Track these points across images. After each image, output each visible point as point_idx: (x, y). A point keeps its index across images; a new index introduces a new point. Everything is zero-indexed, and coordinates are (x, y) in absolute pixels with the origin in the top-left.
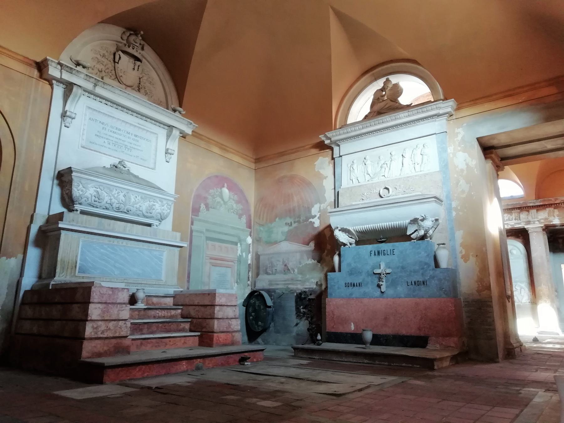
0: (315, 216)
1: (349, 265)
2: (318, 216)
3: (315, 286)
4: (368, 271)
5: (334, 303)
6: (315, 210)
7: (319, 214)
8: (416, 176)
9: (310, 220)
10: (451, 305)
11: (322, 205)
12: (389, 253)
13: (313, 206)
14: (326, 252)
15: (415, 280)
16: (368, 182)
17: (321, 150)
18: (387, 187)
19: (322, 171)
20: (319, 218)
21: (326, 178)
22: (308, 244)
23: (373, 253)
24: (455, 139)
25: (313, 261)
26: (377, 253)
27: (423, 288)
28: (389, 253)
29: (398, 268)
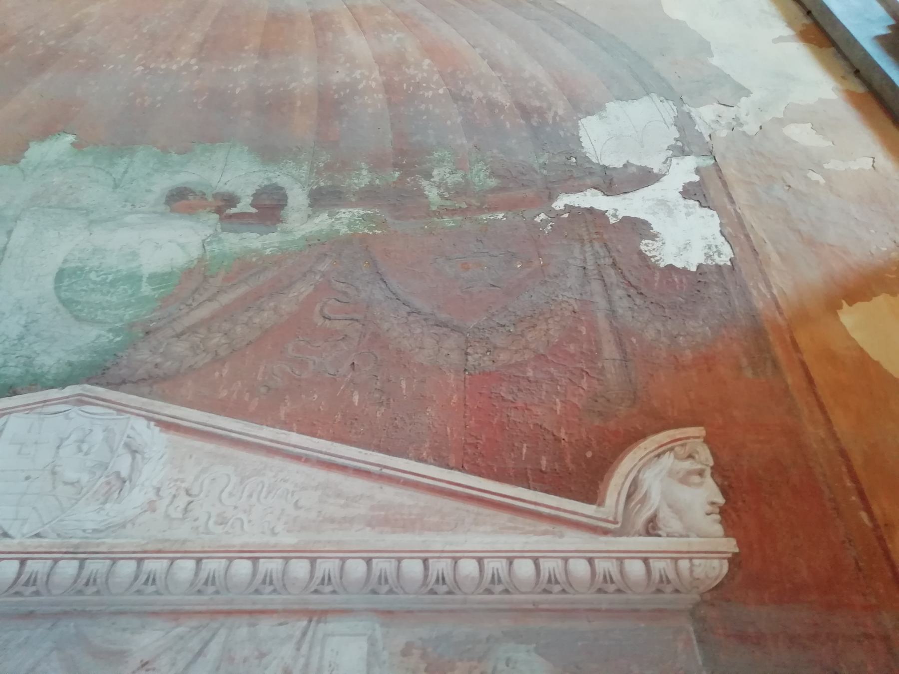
2: (684, 170)
22: (582, 476)
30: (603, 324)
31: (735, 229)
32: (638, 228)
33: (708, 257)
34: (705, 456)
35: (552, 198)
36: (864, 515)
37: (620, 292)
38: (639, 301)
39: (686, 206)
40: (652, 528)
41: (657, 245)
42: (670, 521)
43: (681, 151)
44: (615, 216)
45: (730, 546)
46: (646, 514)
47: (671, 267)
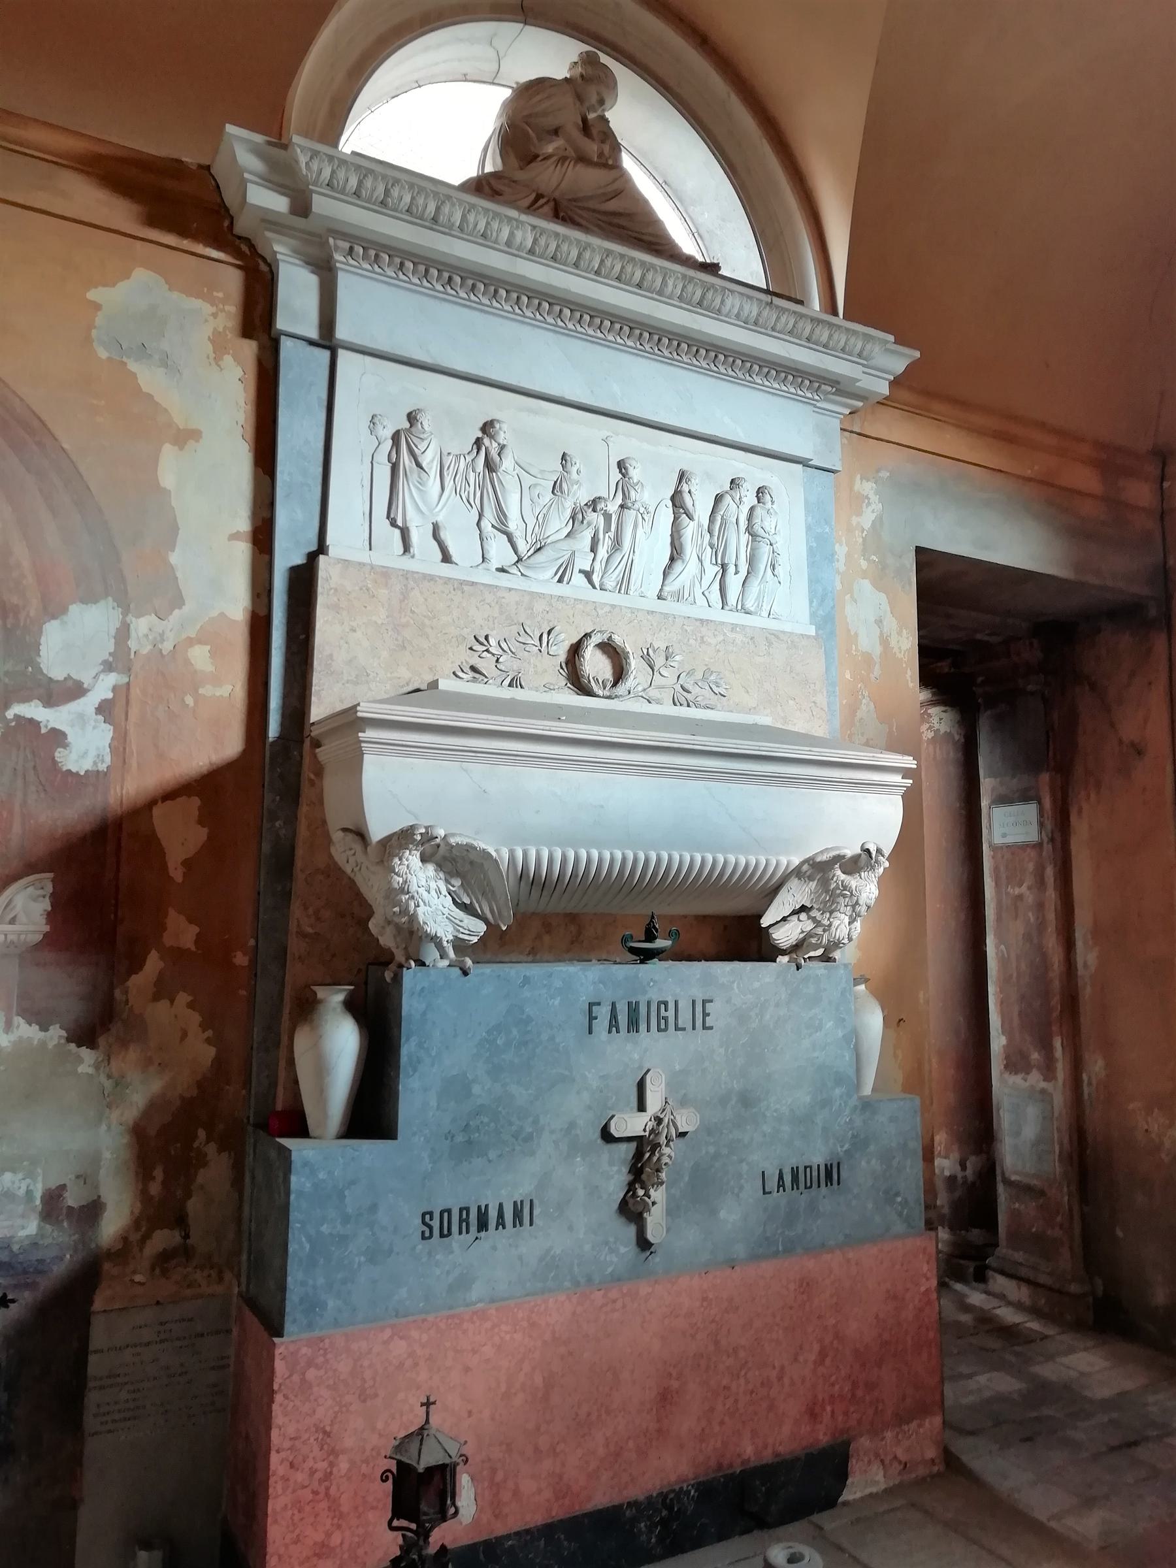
0: (74, 690)
1: (457, 1087)
2: (103, 688)
3: (31, 1227)
4: (572, 1125)
5: (344, 1367)
6: (73, 641)
7: (112, 679)
8: (734, 627)
9: (19, 709)
10: (925, 1268)
11: (142, 625)
12: (685, 1018)
13: (54, 610)
14: (153, 963)
15: (794, 1162)
16: (503, 580)
17: (153, 220)
18: (617, 639)
19: (149, 378)
20: (104, 709)
21: (185, 437)
23: (603, 1013)
24: (855, 520)
25: (27, 1031)
26: (623, 1019)
27: (825, 1198)
28: (685, 1018)
29: (724, 1101)
30: (17, 808)
31: (119, 746)
32: (58, 737)
33: (95, 763)
34: (50, 888)
35: (7, 706)
36: (112, 916)
37: (33, 788)
38: (42, 795)
39: (96, 721)
40: (13, 921)
41: (66, 752)
42: (22, 918)
43: (108, 667)
44: (46, 726)
45: (47, 928)
46: (11, 916)
47: (69, 771)
